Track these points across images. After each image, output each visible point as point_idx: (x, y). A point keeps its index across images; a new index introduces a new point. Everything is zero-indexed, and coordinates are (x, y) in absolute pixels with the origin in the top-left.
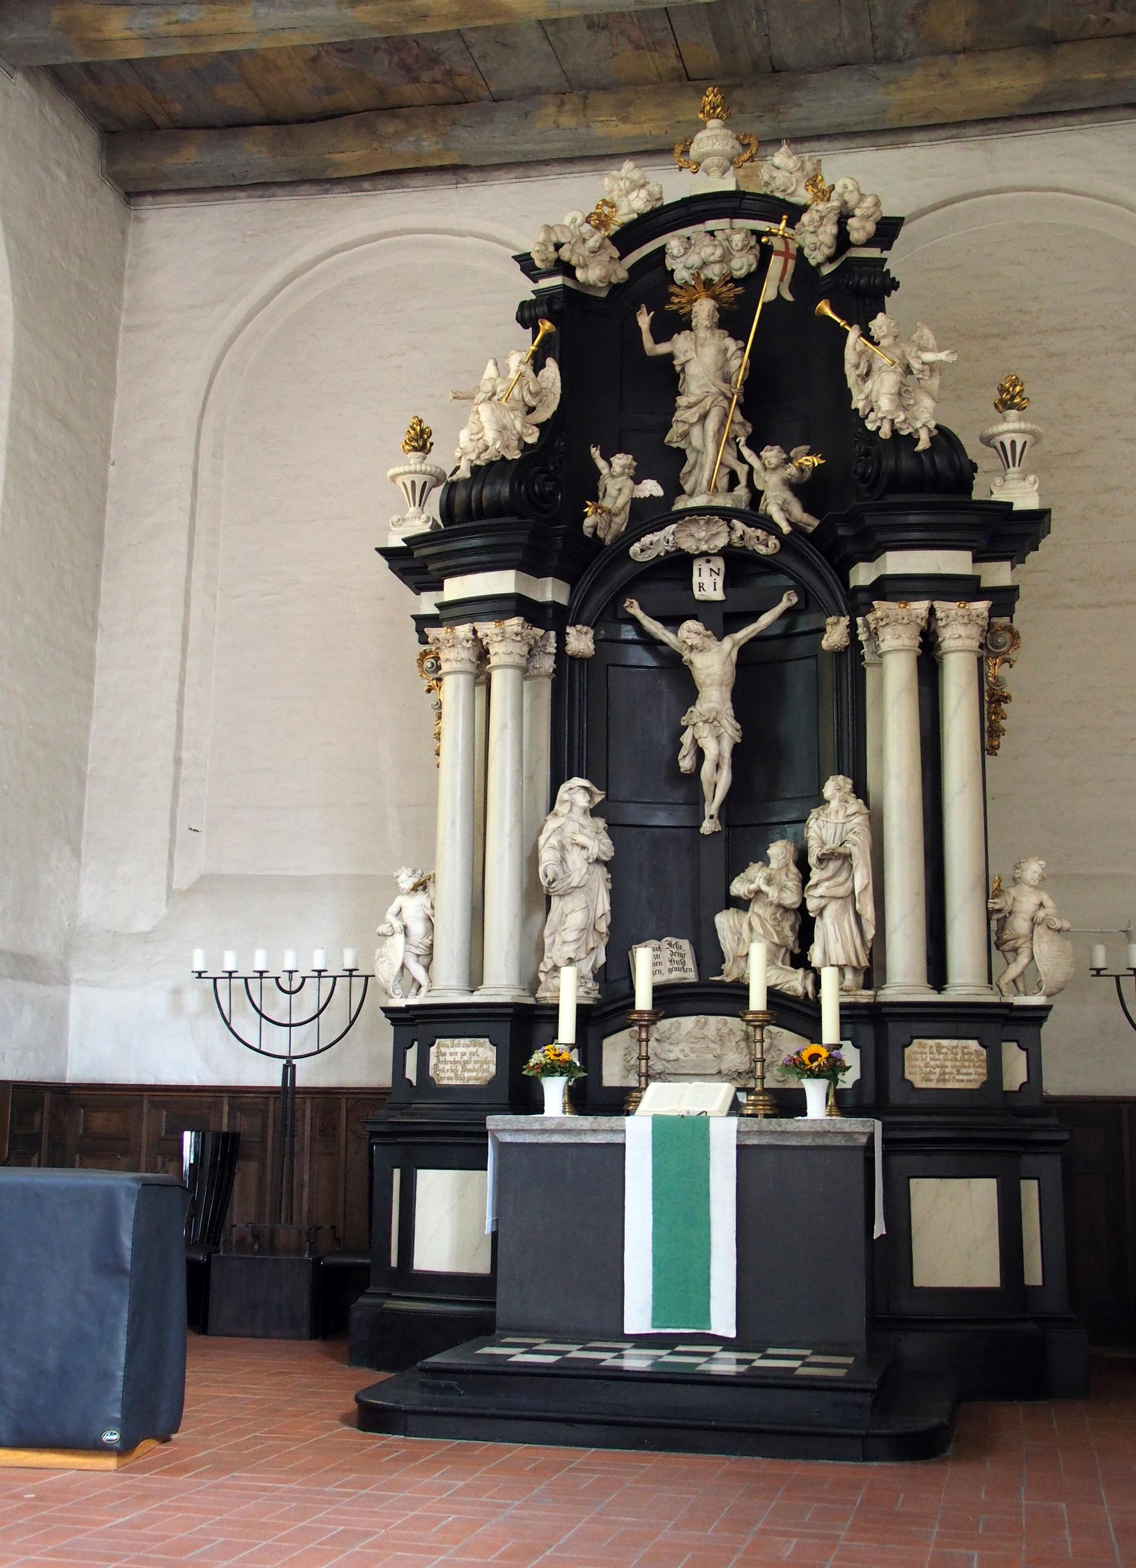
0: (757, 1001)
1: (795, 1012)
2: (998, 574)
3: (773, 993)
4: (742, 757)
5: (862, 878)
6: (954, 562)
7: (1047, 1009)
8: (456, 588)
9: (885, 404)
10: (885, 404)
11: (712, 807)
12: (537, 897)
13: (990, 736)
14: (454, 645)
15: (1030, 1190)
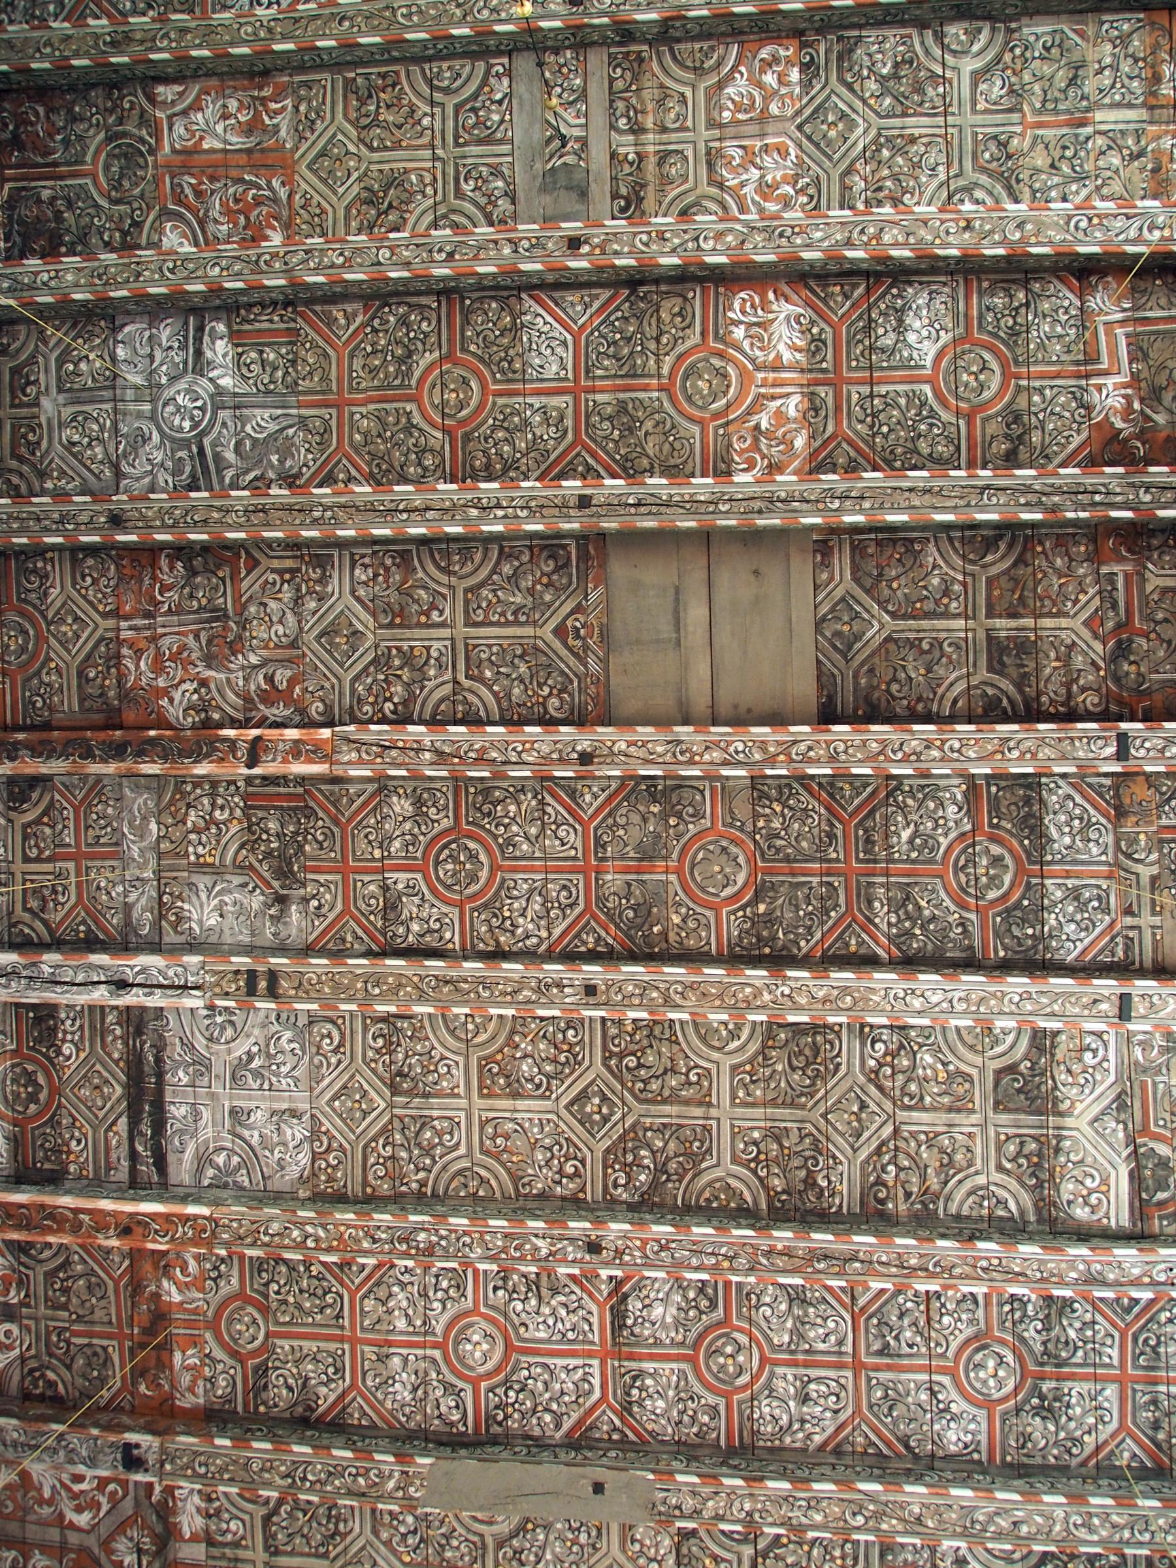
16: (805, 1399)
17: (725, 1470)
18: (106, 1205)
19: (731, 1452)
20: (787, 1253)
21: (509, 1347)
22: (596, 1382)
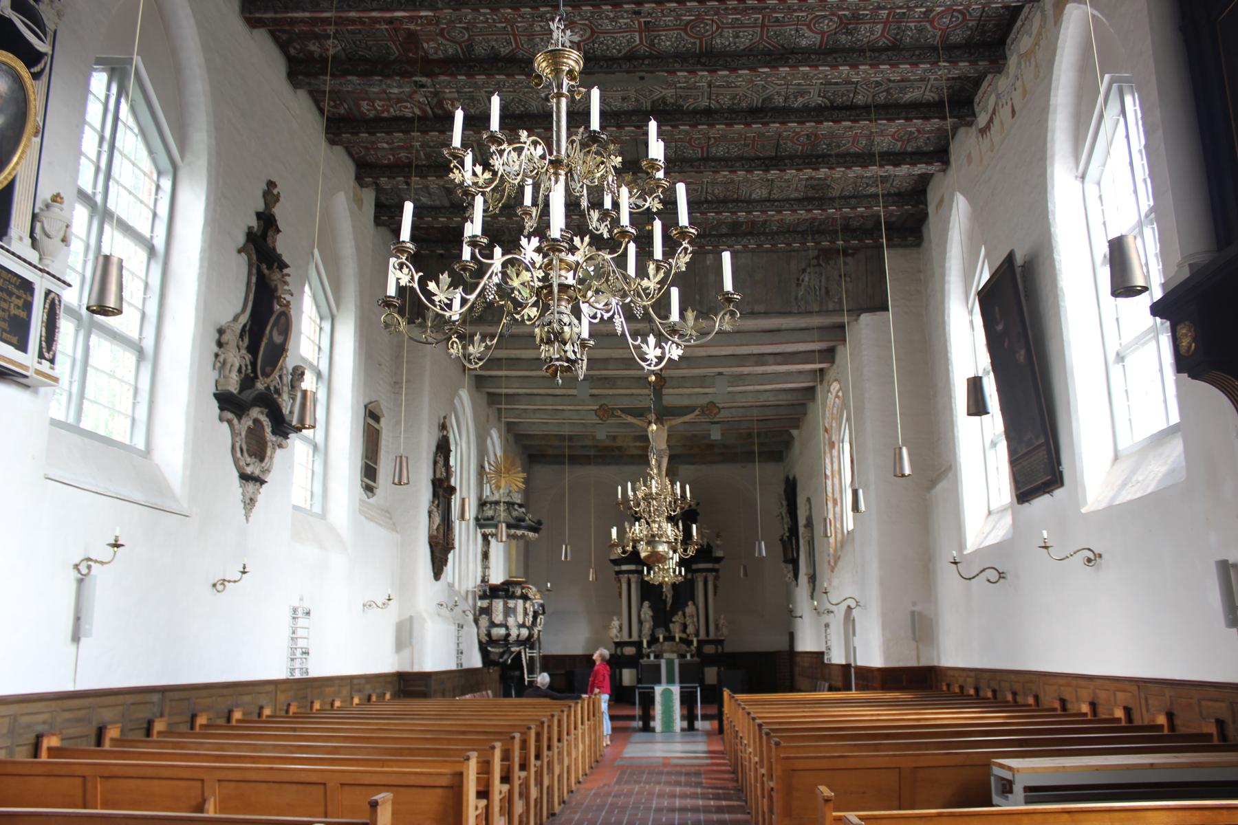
2: (717, 566)
4: (674, 597)
6: (709, 566)
8: (624, 568)
12: (640, 622)
13: (715, 593)
14: (624, 579)
16: (738, 37)
17: (699, 67)
18: (375, 14)
19: (701, 54)
20: (734, 9)
21: (593, 32)
22: (637, 39)
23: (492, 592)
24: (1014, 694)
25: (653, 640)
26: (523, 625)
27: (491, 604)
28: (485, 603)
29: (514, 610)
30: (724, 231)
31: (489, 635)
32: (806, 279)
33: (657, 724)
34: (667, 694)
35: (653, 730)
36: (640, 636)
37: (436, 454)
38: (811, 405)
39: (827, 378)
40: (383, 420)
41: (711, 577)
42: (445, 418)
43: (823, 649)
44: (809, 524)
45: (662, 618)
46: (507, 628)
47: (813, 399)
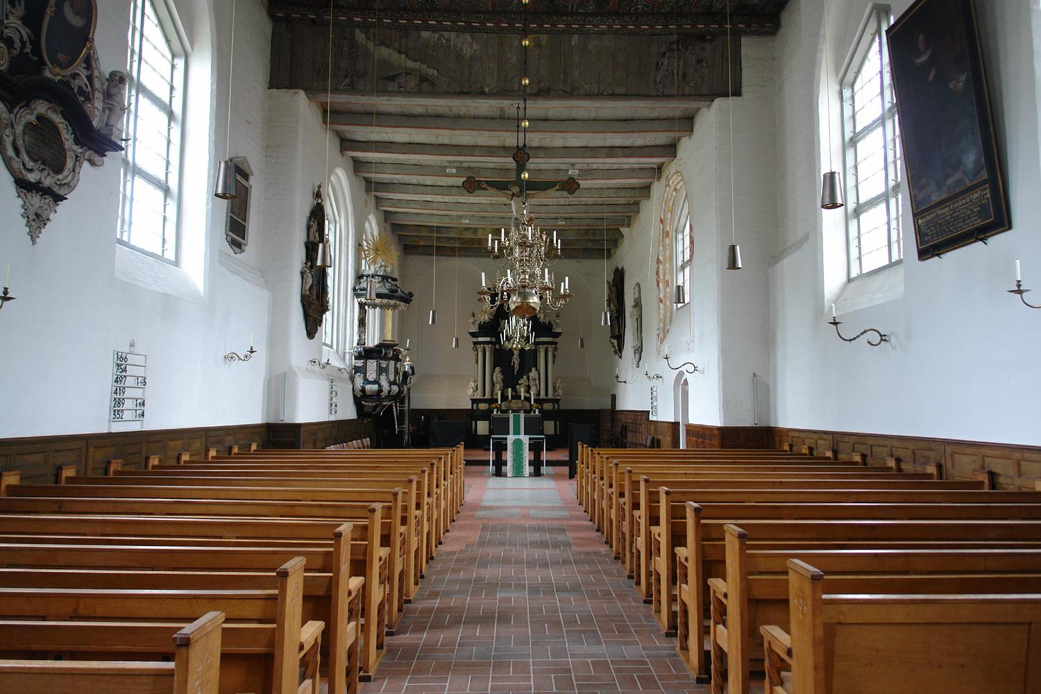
0: (522, 398)
1: (528, 399)
2: (556, 340)
3: (525, 397)
4: (520, 364)
5: (537, 382)
6: (550, 339)
7: (559, 399)
8: (481, 339)
9: (542, 318)
10: (542, 318)
11: (516, 371)
12: (493, 384)
13: (554, 361)
14: (480, 348)
15: (558, 422)
23: (367, 354)
24: (898, 461)
25: (504, 398)
26: (394, 383)
27: (365, 364)
28: (360, 363)
29: (386, 370)
30: (591, 9)
31: (363, 390)
32: (666, 63)
33: (509, 469)
34: (518, 443)
35: (505, 476)
36: (492, 395)
37: (310, 218)
38: (644, 204)
39: (664, 175)
40: (252, 179)
41: (550, 349)
42: (319, 187)
43: (645, 407)
44: (638, 304)
45: (511, 380)
46: (380, 386)
47: (648, 196)
